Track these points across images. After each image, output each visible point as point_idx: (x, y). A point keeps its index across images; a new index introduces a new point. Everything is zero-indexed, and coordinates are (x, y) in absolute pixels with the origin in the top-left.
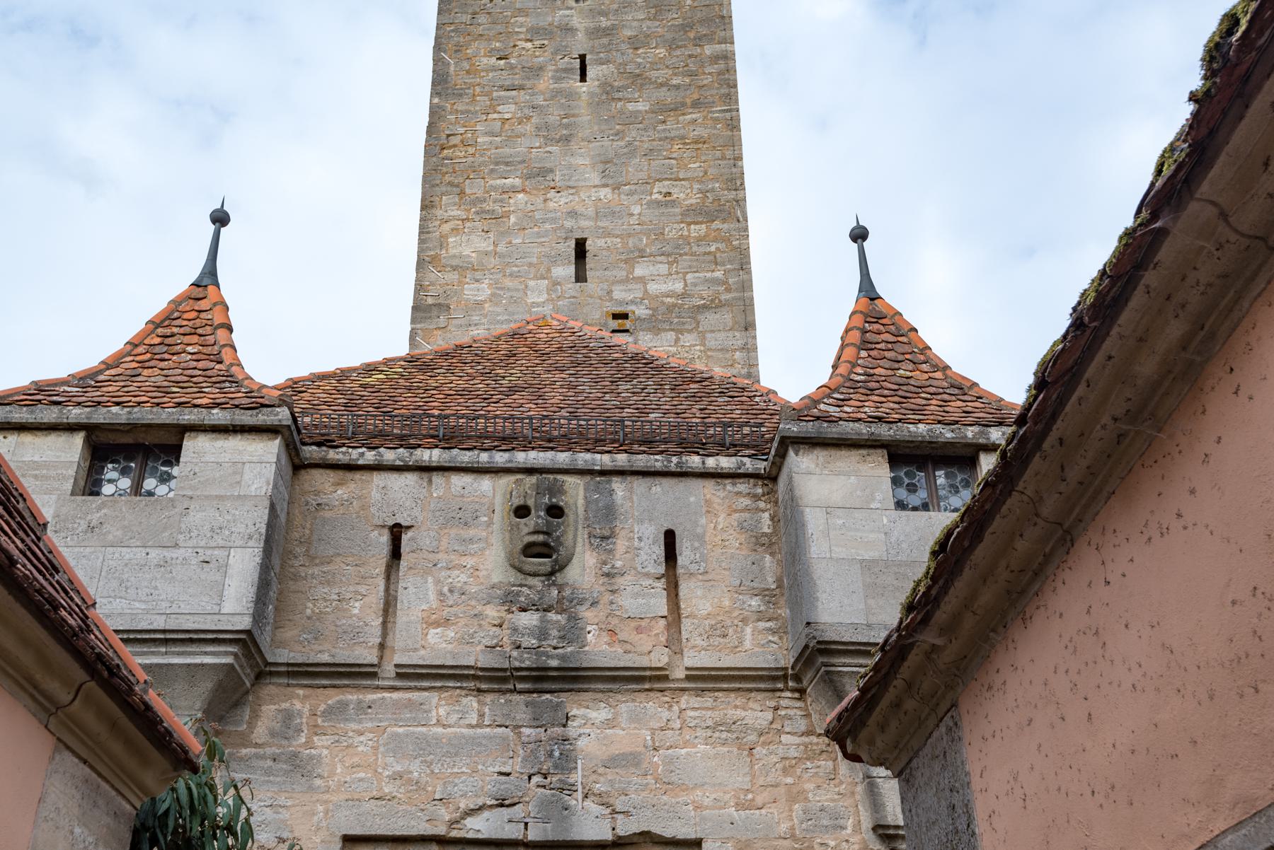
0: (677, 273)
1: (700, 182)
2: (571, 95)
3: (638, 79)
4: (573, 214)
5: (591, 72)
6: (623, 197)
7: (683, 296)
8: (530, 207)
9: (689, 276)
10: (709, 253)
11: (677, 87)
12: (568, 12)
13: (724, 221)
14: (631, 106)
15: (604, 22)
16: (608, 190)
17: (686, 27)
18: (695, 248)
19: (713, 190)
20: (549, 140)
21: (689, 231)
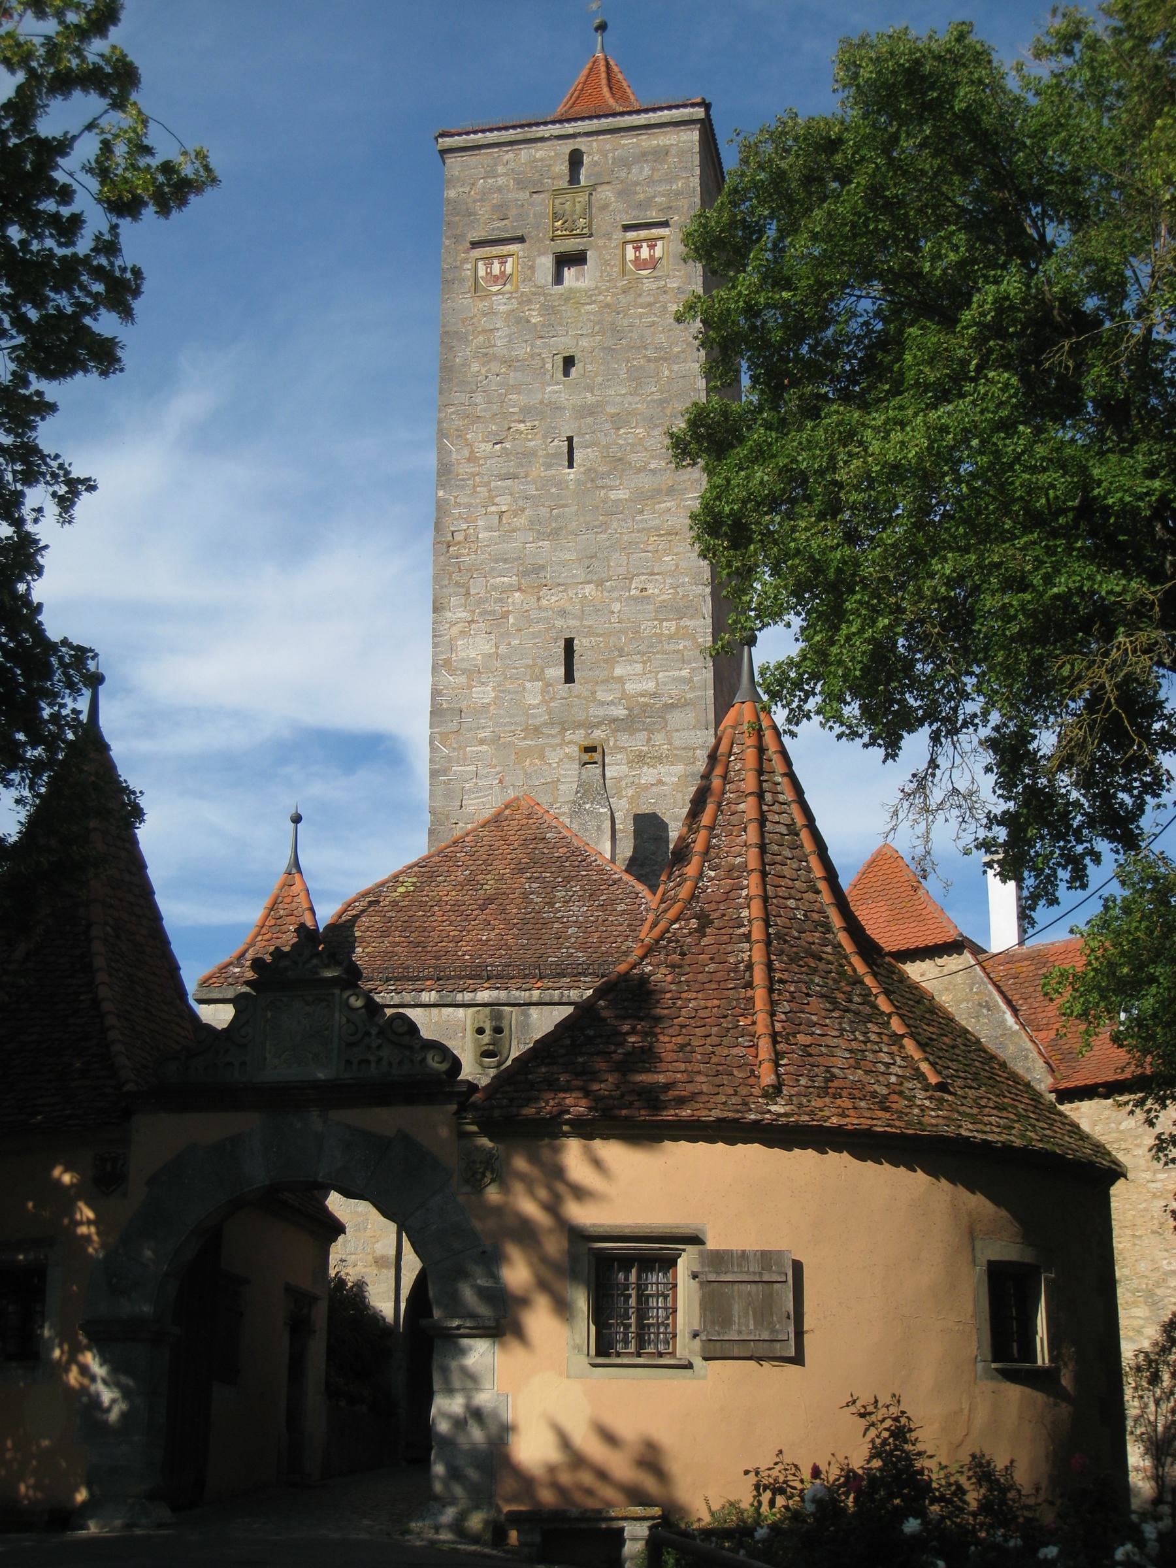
0: (650, 672)
1: (672, 577)
2: (561, 484)
3: (618, 464)
4: (563, 613)
5: (578, 455)
6: (606, 594)
7: (655, 695)
8: (526, 607)
9: (660, 675)
10: (678, 651)
11: (653, 472)
12: (556, 388)
13: (692, 617)
14: (613, 495)
15: (590, 399)
16: (592, 586)
17: (661, 402)
18: (666, 647)
19: (683, 585)
20: (540, 536)
21: (661, 629)
